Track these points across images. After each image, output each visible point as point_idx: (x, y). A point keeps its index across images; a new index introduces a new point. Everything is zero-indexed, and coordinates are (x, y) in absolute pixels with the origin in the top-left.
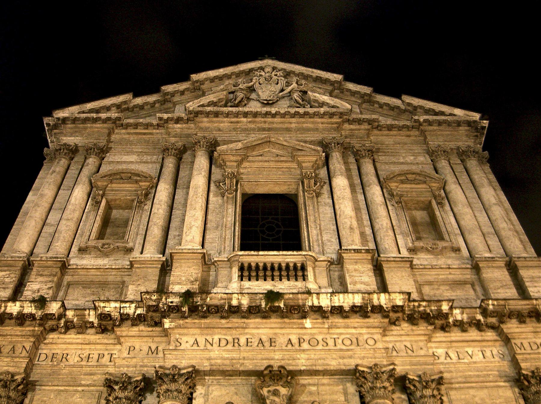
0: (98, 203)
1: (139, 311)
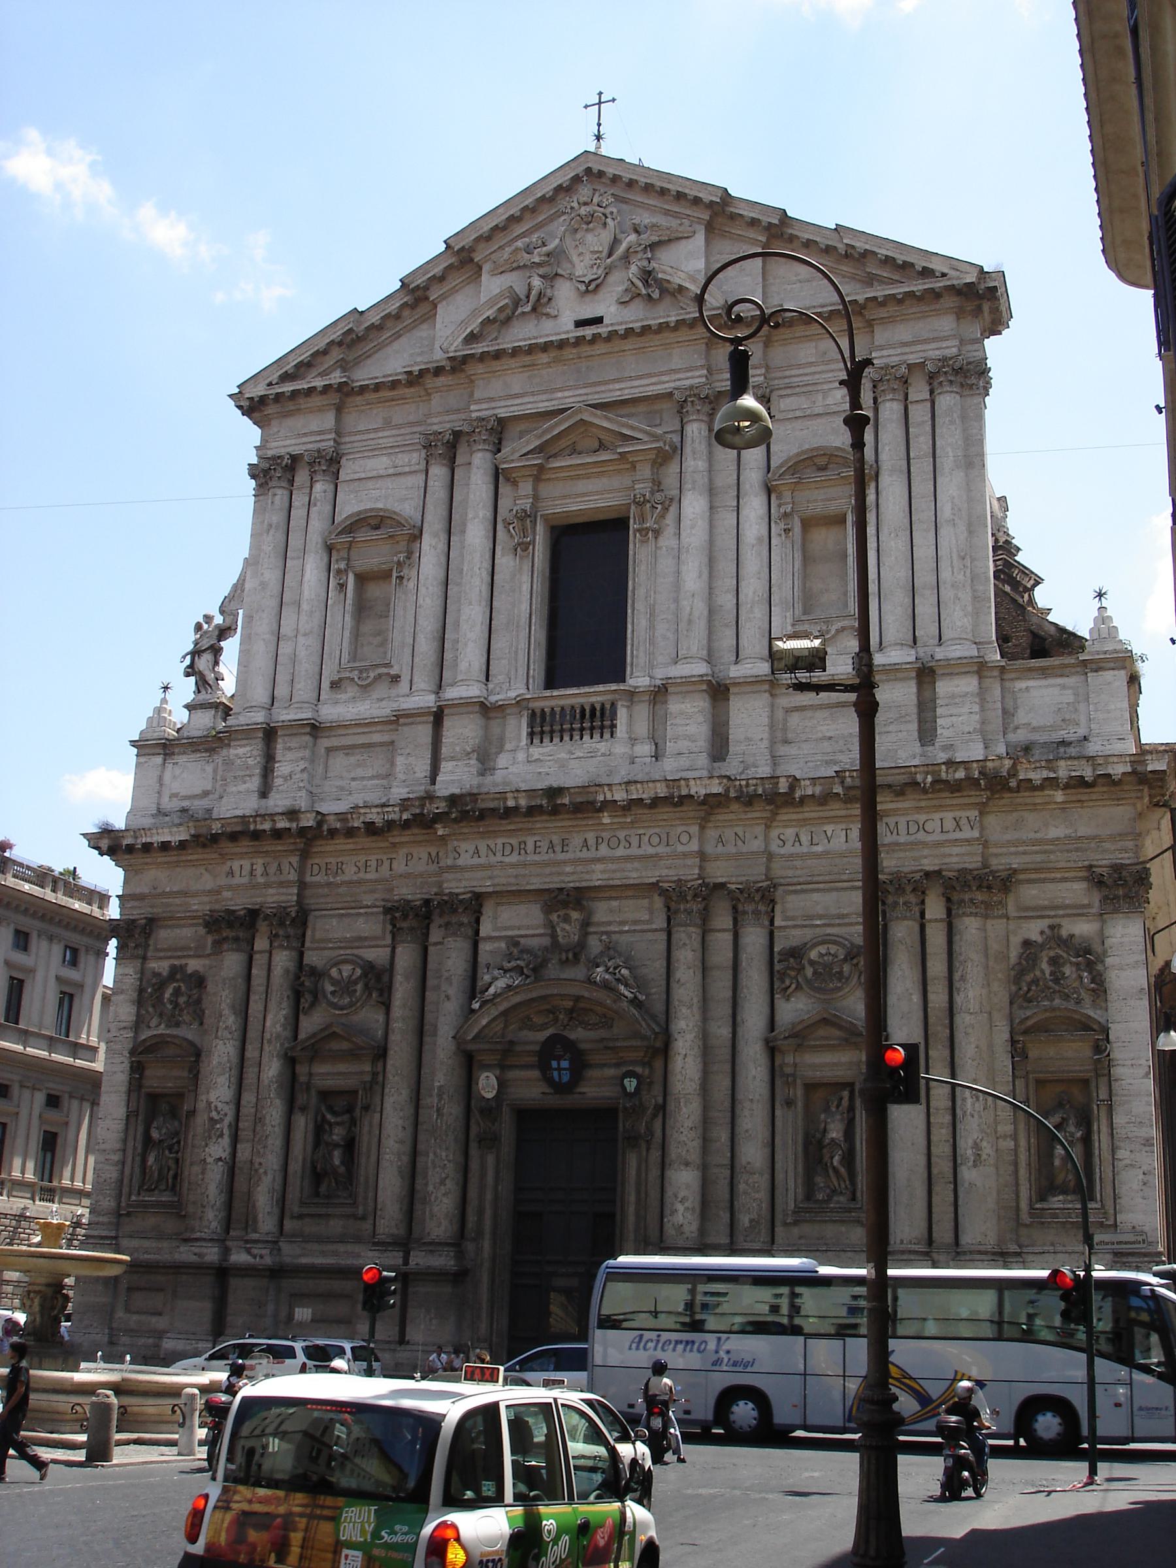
0: (342, 586)
1: (405, 817)
